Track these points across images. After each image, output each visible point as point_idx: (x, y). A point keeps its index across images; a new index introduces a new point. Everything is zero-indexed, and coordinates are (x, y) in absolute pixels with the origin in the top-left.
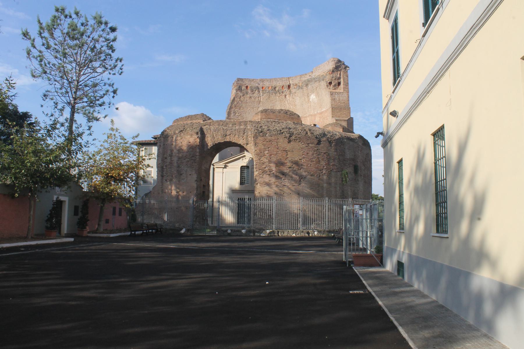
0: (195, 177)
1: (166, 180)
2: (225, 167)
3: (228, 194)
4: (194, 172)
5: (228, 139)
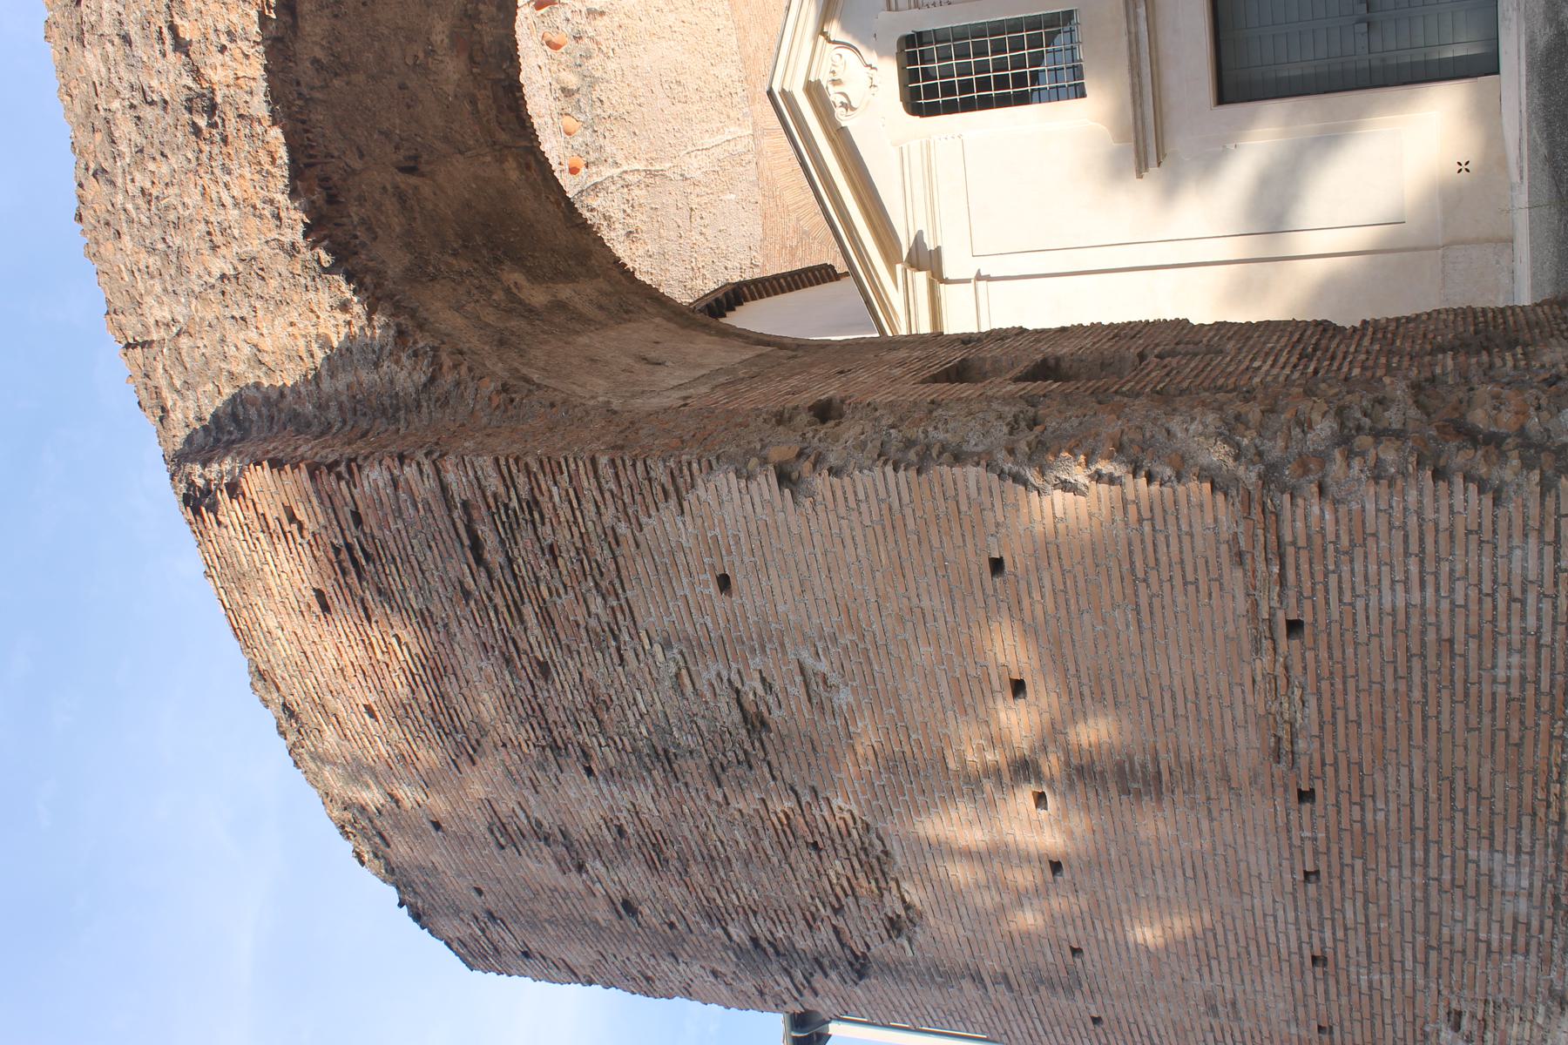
0: (731, 503)
1: (894, 926)
2: (926, 260)
3: (1170, 191)
4: (664, 523)
5: (241, 73)
